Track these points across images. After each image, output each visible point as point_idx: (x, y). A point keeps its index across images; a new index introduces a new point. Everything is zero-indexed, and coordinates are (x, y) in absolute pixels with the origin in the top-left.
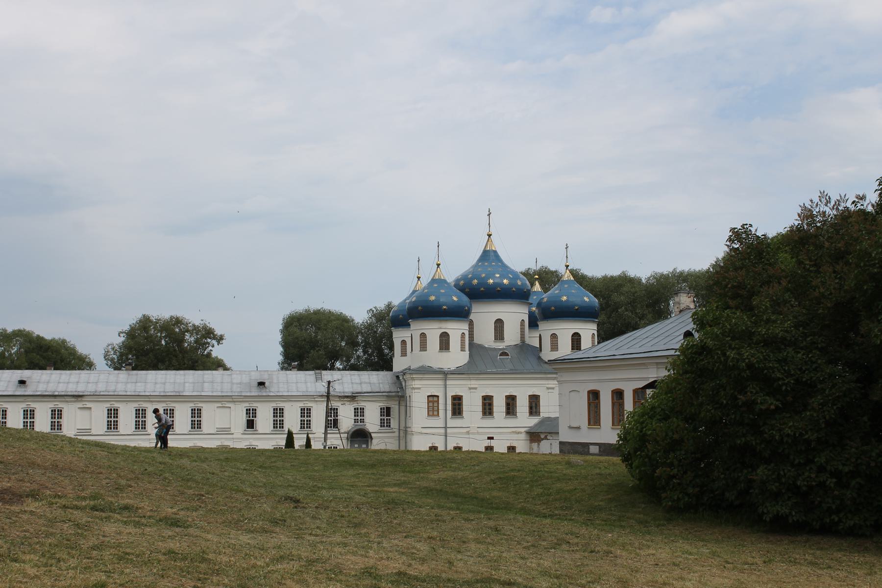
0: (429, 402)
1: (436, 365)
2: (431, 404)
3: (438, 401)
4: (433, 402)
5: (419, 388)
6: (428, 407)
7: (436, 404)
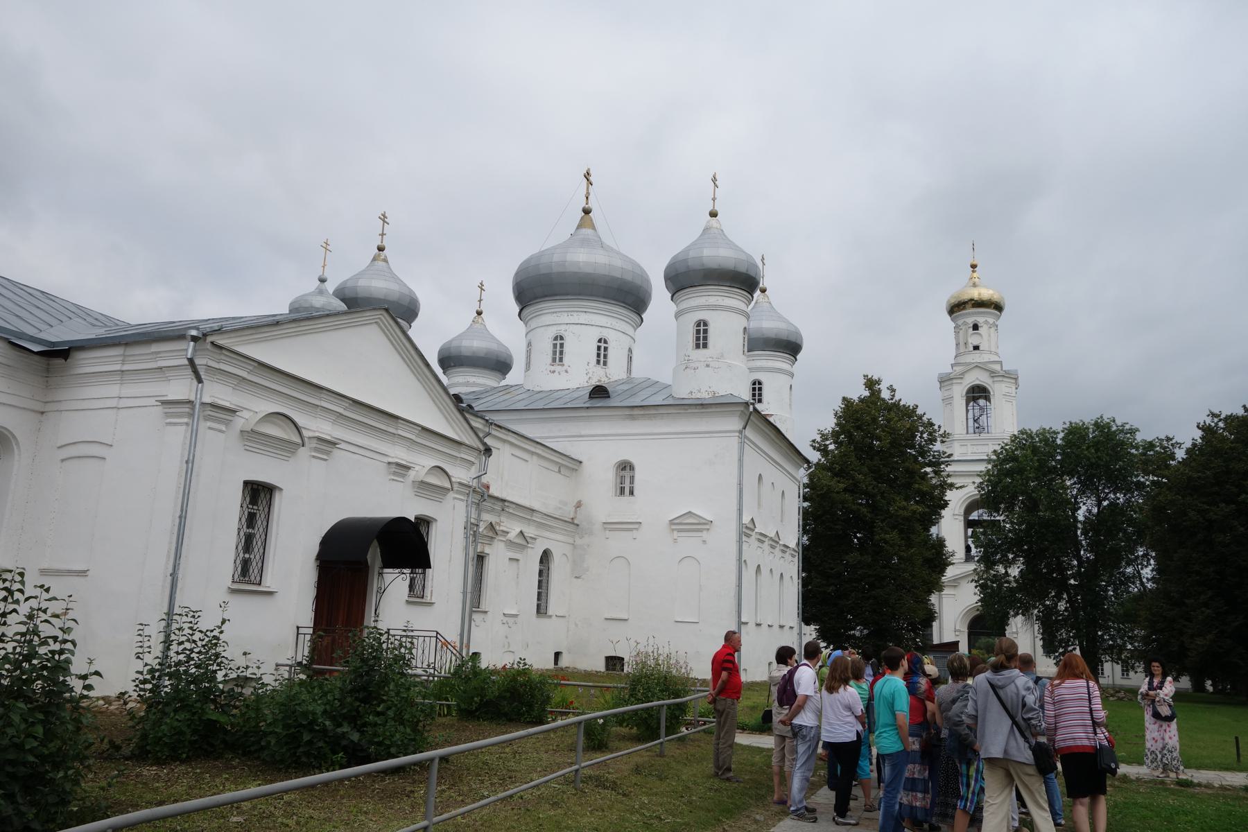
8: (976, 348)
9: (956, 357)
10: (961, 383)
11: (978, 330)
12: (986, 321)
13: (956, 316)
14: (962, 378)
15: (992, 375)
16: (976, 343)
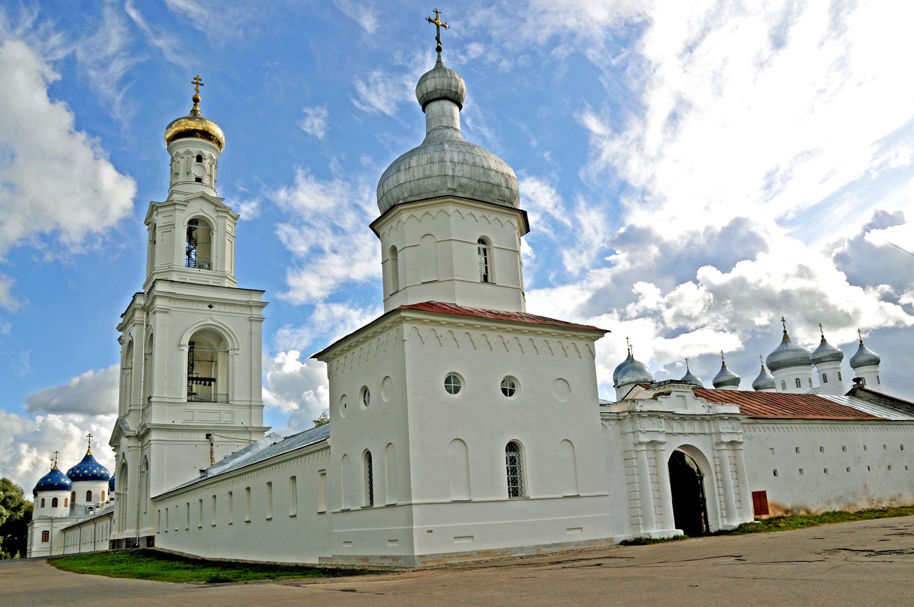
0: (43, 534)
1: (49, 515)
2: (44, 536)
3: (48, 534)
4: (46, 534)
5: (38, 528)
6: (43, 537)
7: (47, 536)
8: (199, 180)
10: (184, 210)
11: (201, 162)
13: (182, 142)
15: (218, 209)
16: (199, 175)
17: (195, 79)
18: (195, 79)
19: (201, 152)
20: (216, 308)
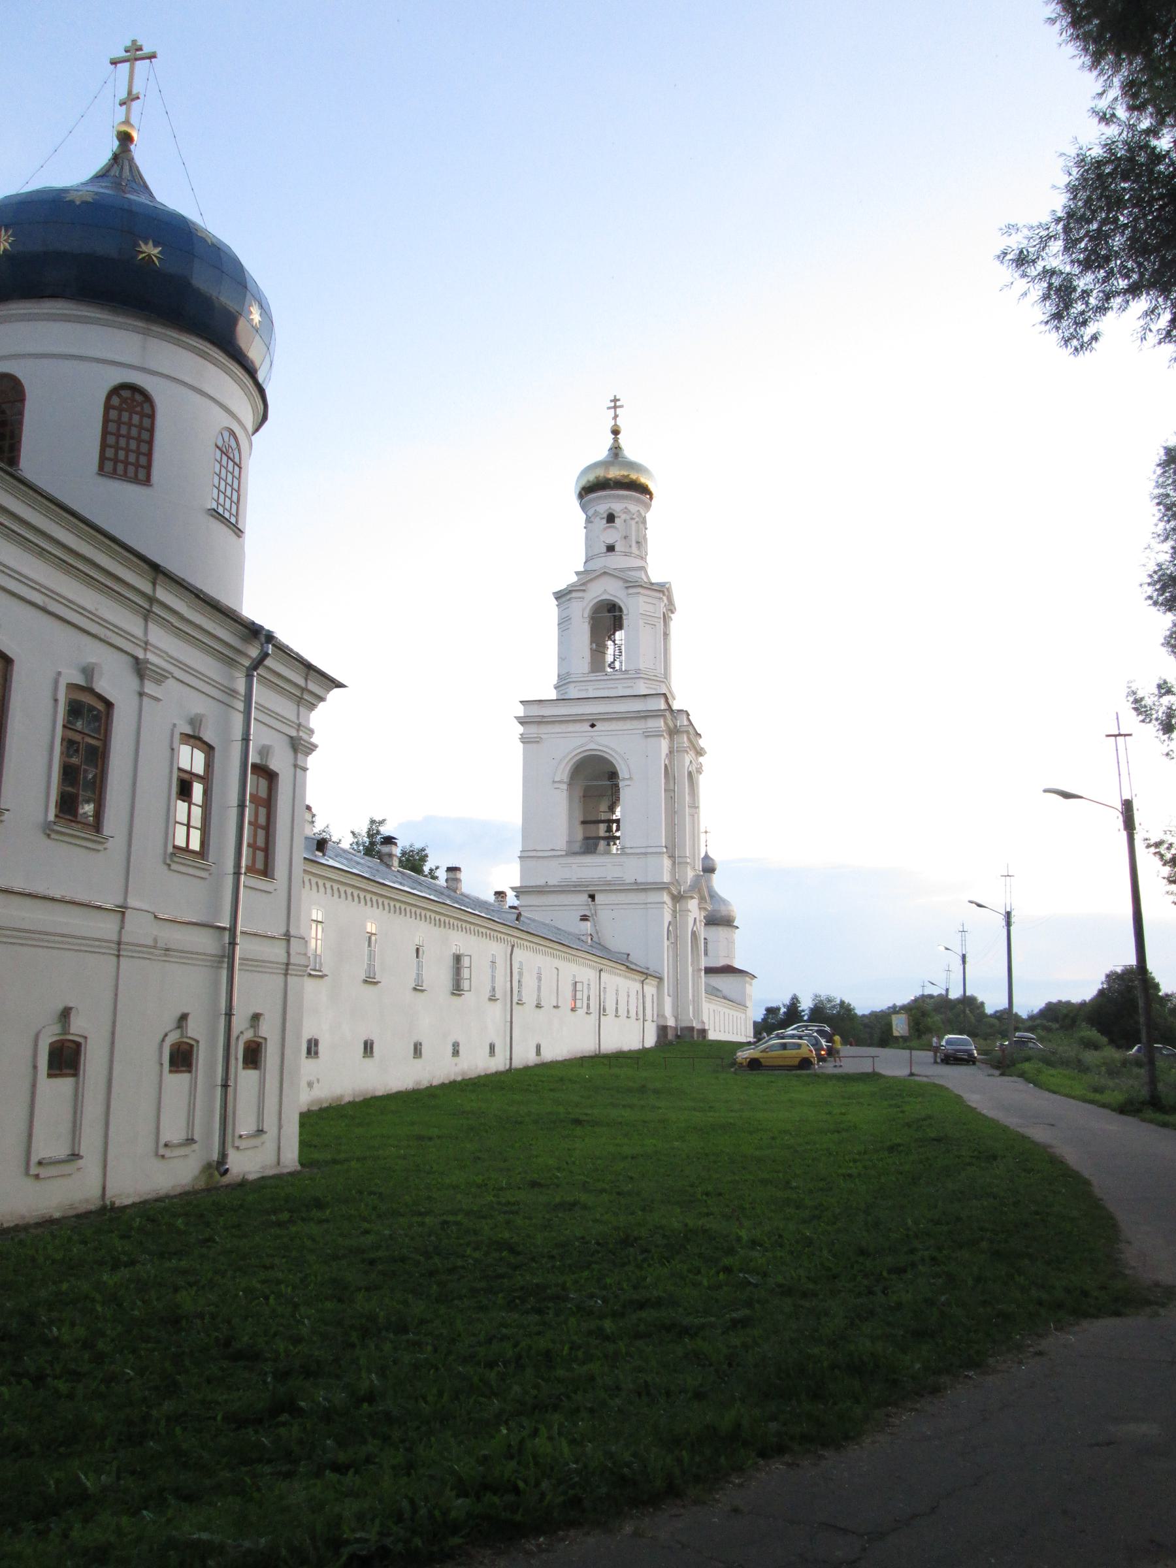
8: (611, 549)
9: (585, 562)
12: (626, 508)
14: (584, 591)
16: (610, 541)
17: (611, 401)
18: (611, 401)
19: (612, 507)
20: (599, 726)
